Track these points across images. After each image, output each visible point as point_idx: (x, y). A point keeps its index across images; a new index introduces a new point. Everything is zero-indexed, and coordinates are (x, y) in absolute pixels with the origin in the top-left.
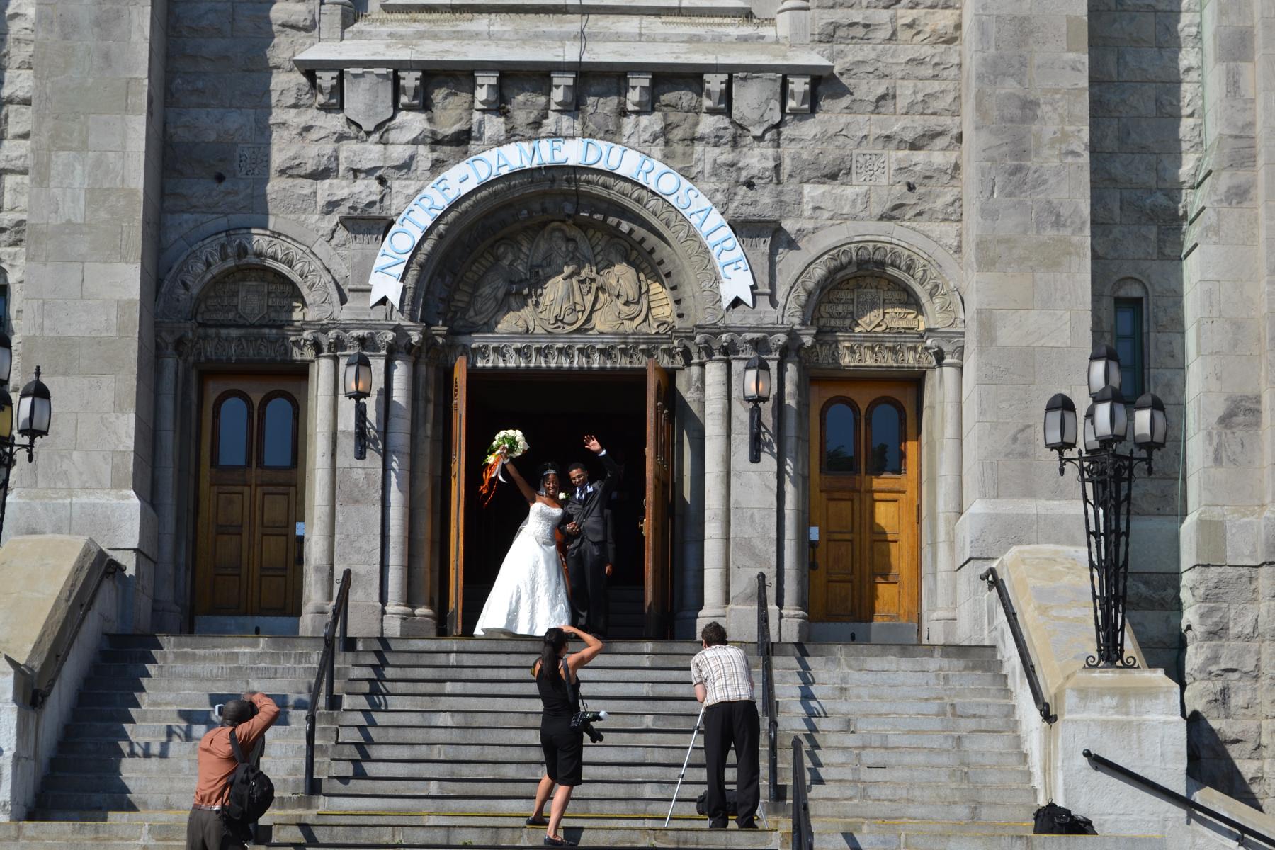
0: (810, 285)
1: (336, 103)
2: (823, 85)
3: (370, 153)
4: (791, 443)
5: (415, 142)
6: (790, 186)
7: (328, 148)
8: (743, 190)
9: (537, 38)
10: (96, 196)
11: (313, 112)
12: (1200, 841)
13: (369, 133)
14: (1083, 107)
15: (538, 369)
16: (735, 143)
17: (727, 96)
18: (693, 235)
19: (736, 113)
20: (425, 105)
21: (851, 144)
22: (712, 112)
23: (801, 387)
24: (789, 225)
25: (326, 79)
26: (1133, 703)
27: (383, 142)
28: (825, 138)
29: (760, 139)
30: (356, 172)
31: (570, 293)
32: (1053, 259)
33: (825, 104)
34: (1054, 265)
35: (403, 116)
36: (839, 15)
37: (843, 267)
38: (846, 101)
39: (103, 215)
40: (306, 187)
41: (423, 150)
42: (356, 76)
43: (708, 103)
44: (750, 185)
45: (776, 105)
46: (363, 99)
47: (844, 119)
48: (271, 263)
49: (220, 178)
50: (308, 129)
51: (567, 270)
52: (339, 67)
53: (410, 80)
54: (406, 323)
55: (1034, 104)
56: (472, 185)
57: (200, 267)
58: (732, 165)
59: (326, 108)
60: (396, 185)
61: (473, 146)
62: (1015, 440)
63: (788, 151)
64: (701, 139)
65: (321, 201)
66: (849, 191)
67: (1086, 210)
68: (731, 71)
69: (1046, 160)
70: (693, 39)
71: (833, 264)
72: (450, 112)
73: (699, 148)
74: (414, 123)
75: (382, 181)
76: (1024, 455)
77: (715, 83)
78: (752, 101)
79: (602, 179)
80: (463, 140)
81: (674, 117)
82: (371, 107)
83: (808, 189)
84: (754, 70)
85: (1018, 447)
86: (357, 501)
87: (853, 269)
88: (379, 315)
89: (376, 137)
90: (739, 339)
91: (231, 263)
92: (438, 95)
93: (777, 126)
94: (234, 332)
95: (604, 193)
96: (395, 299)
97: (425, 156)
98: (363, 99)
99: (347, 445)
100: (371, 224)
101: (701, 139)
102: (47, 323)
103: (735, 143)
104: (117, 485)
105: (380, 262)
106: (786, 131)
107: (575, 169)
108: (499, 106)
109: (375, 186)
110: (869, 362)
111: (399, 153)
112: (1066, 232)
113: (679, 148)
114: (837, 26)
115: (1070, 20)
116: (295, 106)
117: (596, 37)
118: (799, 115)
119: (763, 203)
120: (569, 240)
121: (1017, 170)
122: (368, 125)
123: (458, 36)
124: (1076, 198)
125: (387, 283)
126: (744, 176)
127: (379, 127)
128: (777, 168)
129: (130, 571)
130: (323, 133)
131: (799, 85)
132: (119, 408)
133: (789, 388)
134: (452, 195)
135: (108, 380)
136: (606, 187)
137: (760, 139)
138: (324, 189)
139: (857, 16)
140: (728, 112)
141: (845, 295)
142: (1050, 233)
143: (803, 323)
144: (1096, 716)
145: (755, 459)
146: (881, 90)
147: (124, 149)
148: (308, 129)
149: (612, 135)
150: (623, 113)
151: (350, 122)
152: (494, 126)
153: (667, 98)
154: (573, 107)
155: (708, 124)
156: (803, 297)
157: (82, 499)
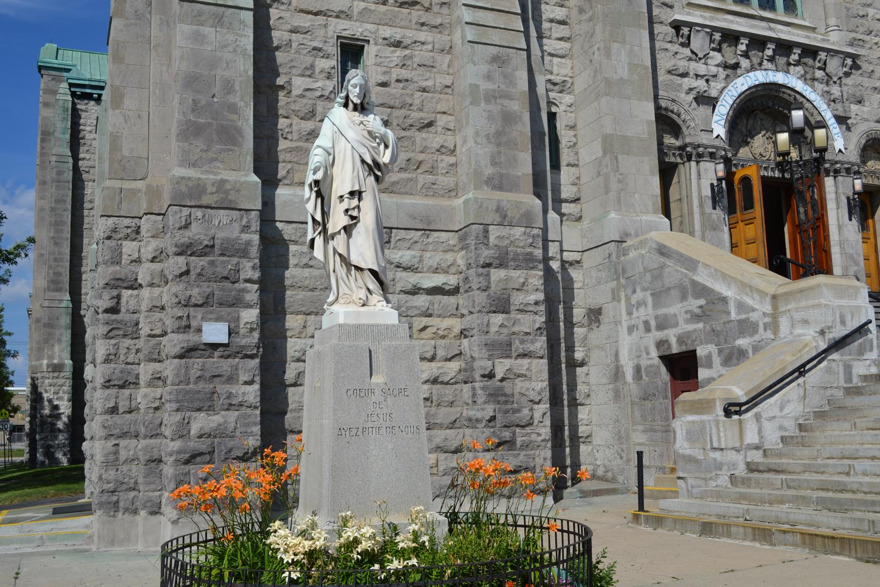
1: (687, 44)
3: (701, 68)
5: (718, 65)
6: (847, 104)
8: (832, 103)
9: (753, 26)
10: (632, 67)
11: (677, 46)
13: (700, 59)
16: (827, 84)
19: (827, 70)
20: (719, 50)
21: (863, 89)
22: (819, 68)
25: (685, 31)
27: (706, 64)
30: (697, 76)
38: (860, 72)
39: (636, 77)
40: (679, 80)
41: (721, 69)
42: (698, 31)
43: (818, 65)
44: (834, 101)
46: (699, 42)
47: (861, 78)
48: (670, 114)
50: (676, 53)
51: (763, 133)
52: (690, 25)
56: (745, 87)
58: (828, 92)
59: (683, 45)
61: (739, 71)
64: (817, 80)
65: (686, 87)
66: (866, 109)
72: (730, 55)
74: (717, 58)
75: (707, 81)
79: (789, 92)
82: (702, 46)
83: (852, 106)
86: (715, 230)
88: (717, 143)
89: (703, 61)
92: (724, 46)
95: (788, 98)
96: (723, 136)
98: (699, 42)
99: (709, 203)
101: (817, 80)
102: (618, 128)
104: (655, 212)
110: (871, 182)
113: (809, 82)
114: (855, 39)
116: (670, 42)
122: (701, 55)
125: (720, 129)
126: (832, 97)
127: (705, 56)
130: (682, 56)
132: (653, 174)
135: (646, 159)
136: (789, 95)
137: (835, 82)
138: (687, 82)
140: (824, 70)
145: (850, 220)
147: (640, 46)
148: (676, 53)
150: (789, 64)
151: (693, 52)
152: (745, 63)
155: (819, 74)
157: (644, 218)
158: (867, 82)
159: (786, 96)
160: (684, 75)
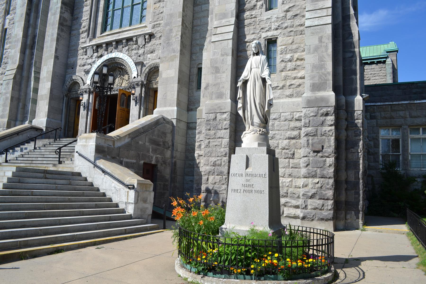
0: (146, 72)
2: (151, 36)
4: (142, 102)
6: (146, 55)
7: (85, 61)
12: (96, 172)
14: (180, 29)
15: (114, 94)
17: (137, 41)
18: (129, 66)
22: (135, 44)
23: (145, 92)
24: (145, 63)
26: (88, 140)
27: (92, 59)
28: (152, 46)
29: (142, 48)
31: (119, 80)
32: (172, 59)
33: (152, 40)
34: (173, 60)
35: (95, 54)
36: (155, 23)
37: (151, 69)
44: (140, 56)
45: (144, 41)
46: (90, 52)
47: (155, 41)
49: (73, 68)
50: (83, 58)
53: (95, 48)
54: (90, 87)
55: (172, 30)
56: (100, 63)
57: (68, 83)
60: (93, 65)
62: (164, 96)
63: (146, 49)
66: (155, 54)
67: (179, 48)
68: (136, 36)
69: (174, 40)
70: (135, 33)
71: (150, 68)
72: (101, 51)
73: (133, 51)
74: (96, 54)
75: (91, 65)
76: (165, 99)
77: (134, 39)
78: (141, 41)
80: (101, 56)
81: (130, 46)
83: (149, 56)
84: (140, 35)
85: (164, 97)
87: (153, 69)
88: (87, 87)
90: (134, 84)
91: (72, 82)
92: (99, 50)
93: (145, 45)
94: (74, 93)
97: (97, 59)
98: (90, 52)
100: (87, 72)
103: (138, 49)
105: (88, 78)
106: (146, 45)
107: (114, 58)
108: (107, 50)
109: (90, 66)
111: (93, 60)
112: (175, 54)
114: (155, 25)
115: (179, 12)
117: (121, 35)
118: (148, 42)
119: (141, 59)
120: (119, 71)
121: (168, 43)
123: (103, 40)
124: (177, 46)
128: (144, 52)
129: (44, 130)
131: (147, 37)
133: (143, 92)
134: (98, 66)
137: (142, 48)
139: (158, 23)
140: (137, 44)
141: (155, 74)
142: (173, 54)
143: (145, 80)
144: (82, 144)
146: (160, 35)
148: (83, 58)
149: (121, 51)
150: (123, 47)
152: (106, 52)
153: (129, 43)
154: (116, 48)
156: (145, 75)
158: (158, 42)
159: (118, 61)
160: (84, 65)
